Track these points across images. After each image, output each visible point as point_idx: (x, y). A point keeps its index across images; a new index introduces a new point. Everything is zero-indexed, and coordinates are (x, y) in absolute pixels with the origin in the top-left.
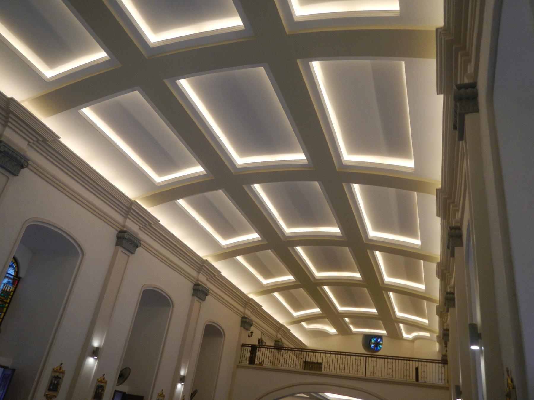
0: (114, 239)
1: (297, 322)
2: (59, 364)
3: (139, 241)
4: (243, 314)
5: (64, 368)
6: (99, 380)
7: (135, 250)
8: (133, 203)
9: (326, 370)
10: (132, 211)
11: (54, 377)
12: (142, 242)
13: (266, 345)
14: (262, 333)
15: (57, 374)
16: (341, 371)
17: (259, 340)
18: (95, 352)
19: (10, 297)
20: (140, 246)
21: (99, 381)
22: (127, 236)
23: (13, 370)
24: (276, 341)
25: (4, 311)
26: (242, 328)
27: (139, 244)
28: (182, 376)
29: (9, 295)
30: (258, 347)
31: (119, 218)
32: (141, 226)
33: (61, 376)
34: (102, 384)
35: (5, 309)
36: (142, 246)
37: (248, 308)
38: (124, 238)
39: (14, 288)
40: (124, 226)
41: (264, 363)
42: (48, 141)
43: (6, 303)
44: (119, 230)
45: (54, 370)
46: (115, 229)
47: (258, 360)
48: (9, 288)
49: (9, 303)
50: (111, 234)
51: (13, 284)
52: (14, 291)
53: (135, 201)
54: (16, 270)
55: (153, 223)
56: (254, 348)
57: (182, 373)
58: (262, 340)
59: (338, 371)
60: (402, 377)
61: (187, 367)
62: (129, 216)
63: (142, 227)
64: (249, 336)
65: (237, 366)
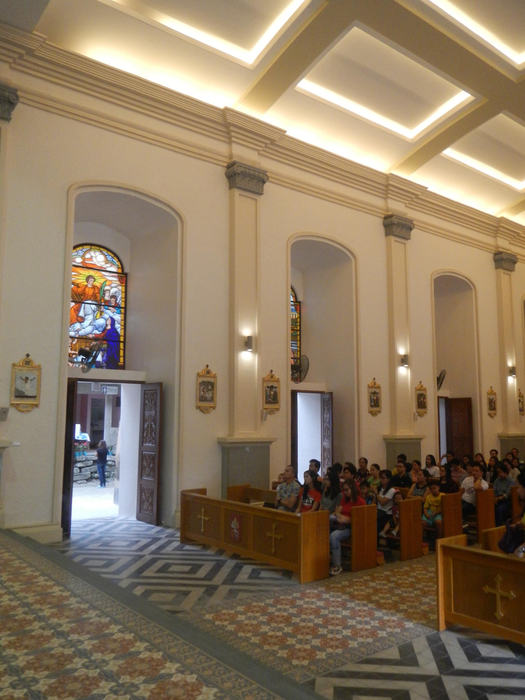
0: (381, 230)
2: (372, 380)
3: (411, 221)
5: (378, 383)
6: (418, 388)
7: (410, 235)
8: (389, 177)
10: (391, 188)
11: (372, 393)
12: (414, 222)
15: (373, 390)
18: (404, 360)
19: (298, 324)
20: (414, 227)
21: (418, 390)
22: (396, 221)
23: (331, 394)
25: (299, 339)
27: (412, 226)
28: (510, 367)
29: (297, 322)
31: (379, 202)
32: (407, 202)
33: (377, 391)
34: (422, 392)
35: (299, 337)
36: (416, 226)
38: (392, 224)
39: (298, 314)
40: (387, 210)
42: (276, 141)
43: (297, 330)
44: (383, 216)
45: (369, 387)
46: (379, 217)
48: (294, 316)
49: (300, 330)
50: (377, 223)
51: (296, 309)
52: (300, 317)
53: (391, 174)
54: (294, 295)
55: (419, 193)
61: (514, 356)
62: (389, 196)
63: (409, 204)
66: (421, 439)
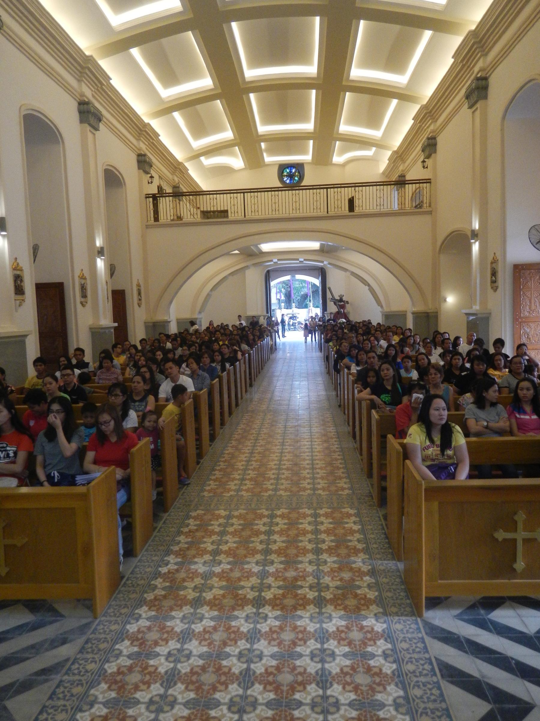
1: (196, 156)
4: (139, 150)
9: (233, 215)
13: (167, 192)
14: (160, 177)
16: (274, 213)
17: (158, 187)
24: (174, 187)
26: (141, 171)
28: (98, 247)
30: (159, 197)
37: (144, 141)
41: (185, 217)
47: (175, 214)
56: (155, 197)
57: (99, 243)
58: (161, 188)
59: (291, 212)
60: (375, 208)
64: (149, 183)
65: (146, 225)
66: (26, 336)
